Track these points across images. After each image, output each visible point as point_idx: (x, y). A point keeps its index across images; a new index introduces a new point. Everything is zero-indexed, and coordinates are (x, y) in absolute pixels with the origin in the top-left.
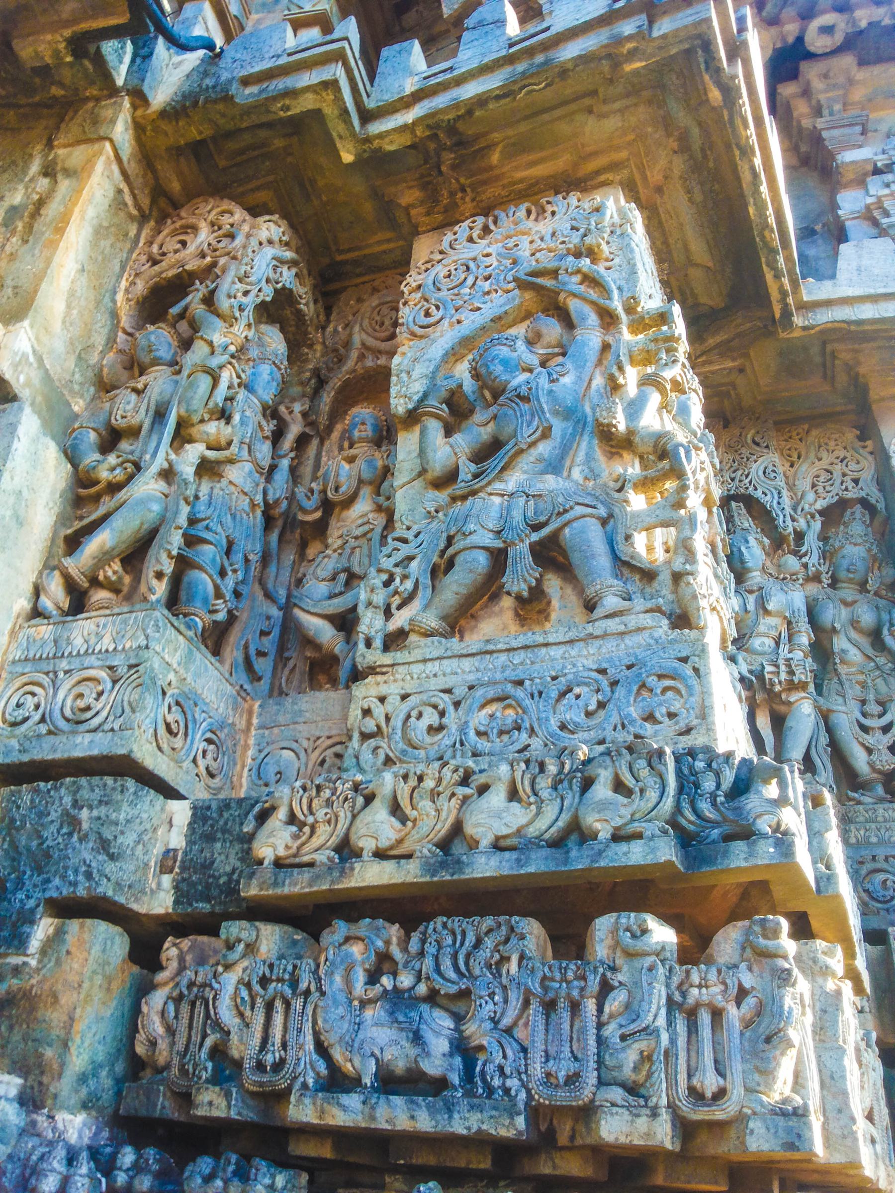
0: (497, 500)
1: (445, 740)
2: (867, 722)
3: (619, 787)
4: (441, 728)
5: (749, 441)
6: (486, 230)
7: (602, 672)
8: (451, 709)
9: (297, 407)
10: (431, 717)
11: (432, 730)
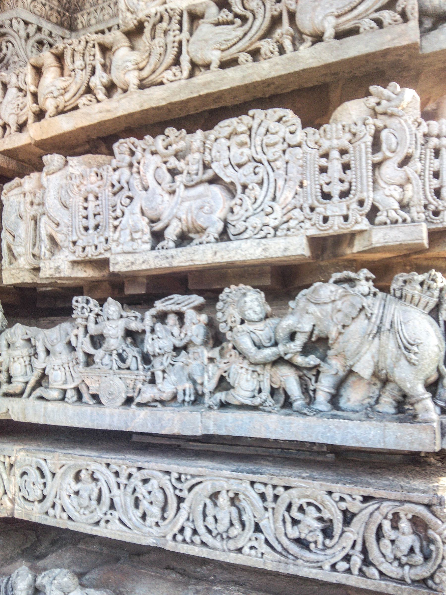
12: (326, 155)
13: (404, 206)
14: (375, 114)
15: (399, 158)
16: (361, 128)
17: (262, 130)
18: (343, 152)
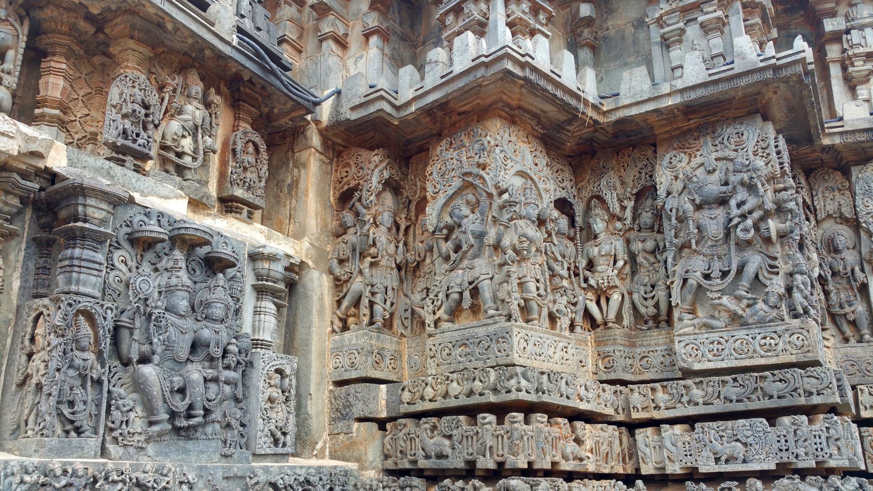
0: (460, 272)
1: (451, 358)
2: (645, 296)
3: (481, 381)
4: (450, 354)
5: (601, 166)
6: (451, 143)
7: (488, 336)
8: (452, 348)
9: (403, 216)
10: (447, 351)
11: (449, 355)
12: (779, 436)
13: (806, 454)
14: (793, 424)
15: (803, 439)
16: (789, 429)
17: (755, 426)
18: (785, 436)
